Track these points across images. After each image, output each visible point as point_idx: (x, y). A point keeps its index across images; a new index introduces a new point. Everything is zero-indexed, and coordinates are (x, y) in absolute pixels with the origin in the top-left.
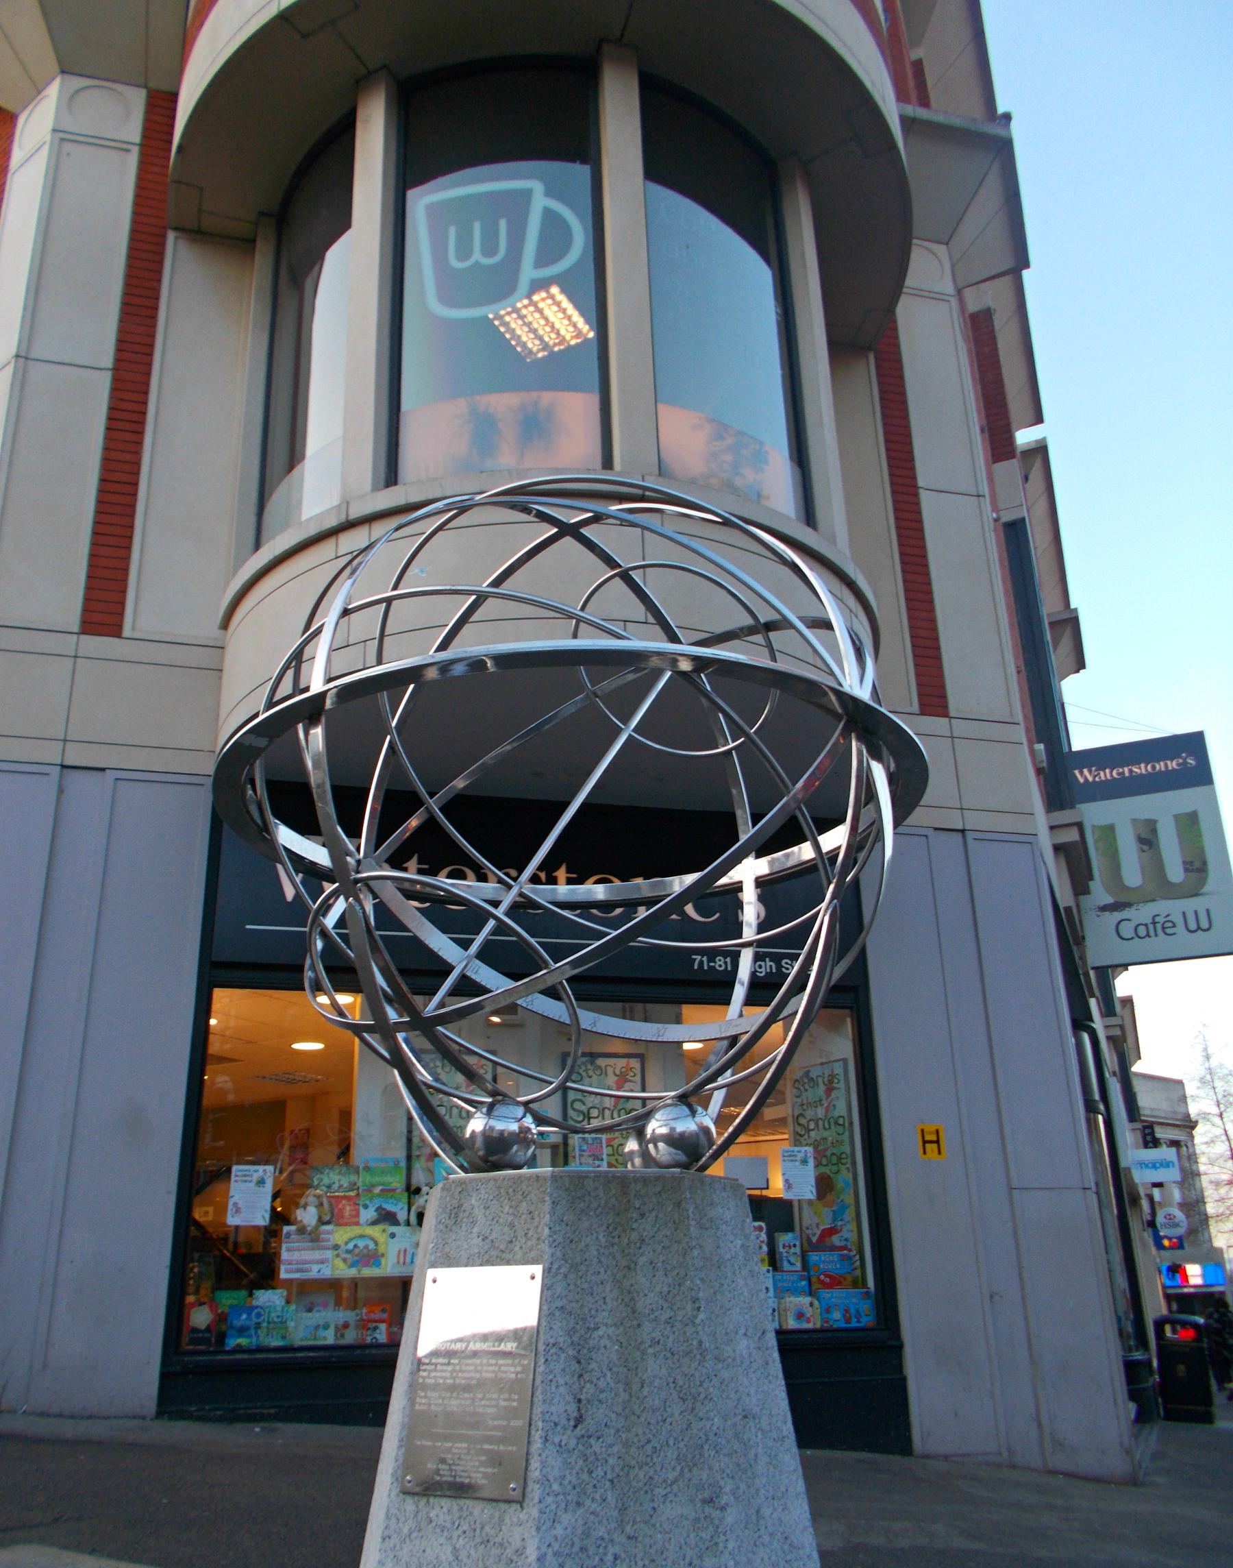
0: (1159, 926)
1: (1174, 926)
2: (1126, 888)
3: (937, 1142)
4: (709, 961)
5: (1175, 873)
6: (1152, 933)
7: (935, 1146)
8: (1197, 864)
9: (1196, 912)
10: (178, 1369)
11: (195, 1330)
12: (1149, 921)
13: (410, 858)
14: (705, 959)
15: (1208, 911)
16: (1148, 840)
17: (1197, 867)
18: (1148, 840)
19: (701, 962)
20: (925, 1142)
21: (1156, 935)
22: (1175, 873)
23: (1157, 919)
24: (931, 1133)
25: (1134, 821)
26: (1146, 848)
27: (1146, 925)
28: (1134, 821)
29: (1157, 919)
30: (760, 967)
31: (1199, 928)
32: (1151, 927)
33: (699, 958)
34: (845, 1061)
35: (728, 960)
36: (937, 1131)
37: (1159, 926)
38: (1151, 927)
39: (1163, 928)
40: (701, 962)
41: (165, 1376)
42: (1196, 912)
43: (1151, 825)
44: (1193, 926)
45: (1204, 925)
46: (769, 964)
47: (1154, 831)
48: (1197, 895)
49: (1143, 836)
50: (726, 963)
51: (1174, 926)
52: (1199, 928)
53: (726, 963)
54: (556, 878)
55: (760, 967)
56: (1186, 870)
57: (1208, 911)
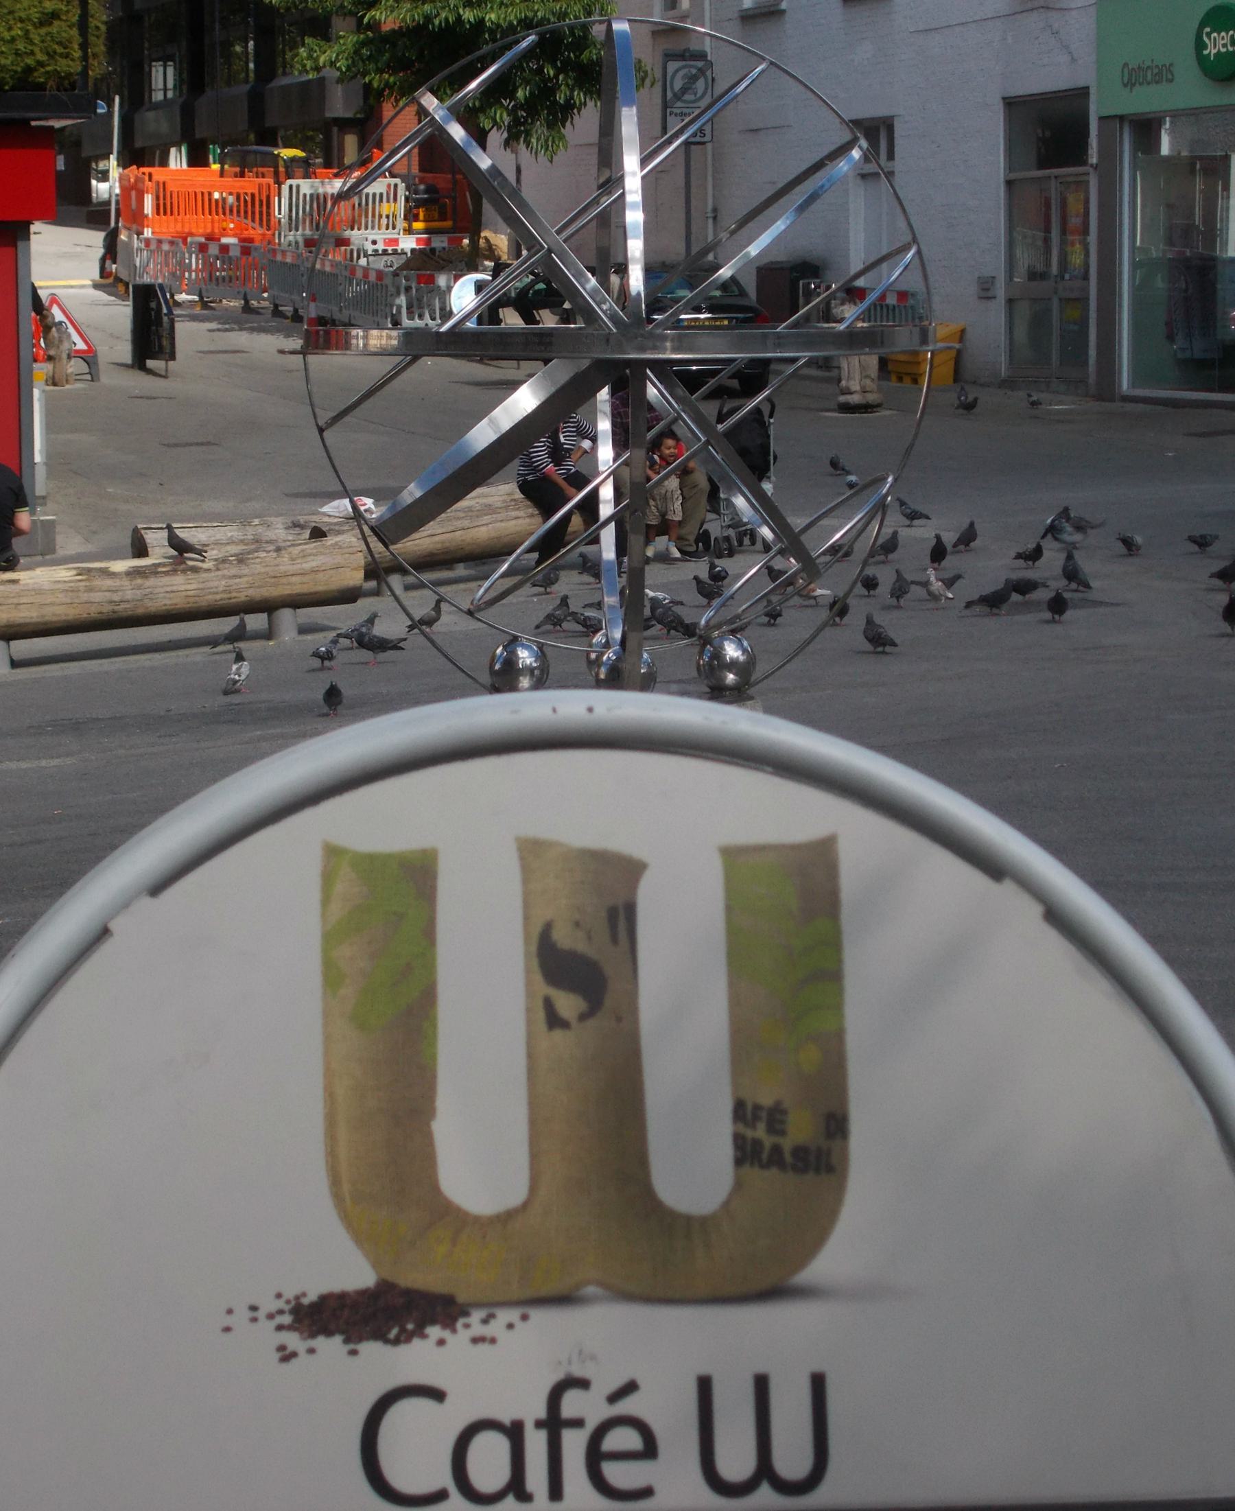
0: (574, 1444)
1: (650, 1450)
2: (445, 1213)
5: (693, 1165)
6: (537, 1478)
8: (801, 1129)
9: (761, 1385)
12: (533, 1408)
15: (818, 1383)
16: (584, 966)
17: (796, 1144)
18: (584, 966)
21: (556, 1492)
22: (693, 1165)
23: (572, 1404)
25: (532, 852)
26: (568, 1004)
27: (515, 1432)
28: (532, 852)
29: (572, 1404)
31: (765, 1471)
32: (536, 1443)
37: (574, 1444)
38: (536, 1443)
39: (595, 1457)
42: (761, 1385)
43: (612, 892)
44: (736, 1460)
45: (792, 1459)
47: (621, 919)
48: (776, 1292)
49: (564, 938)
51: (650, 1450)
52: (765, 1471)
56: (747, 1153)
57: (818, 1383)
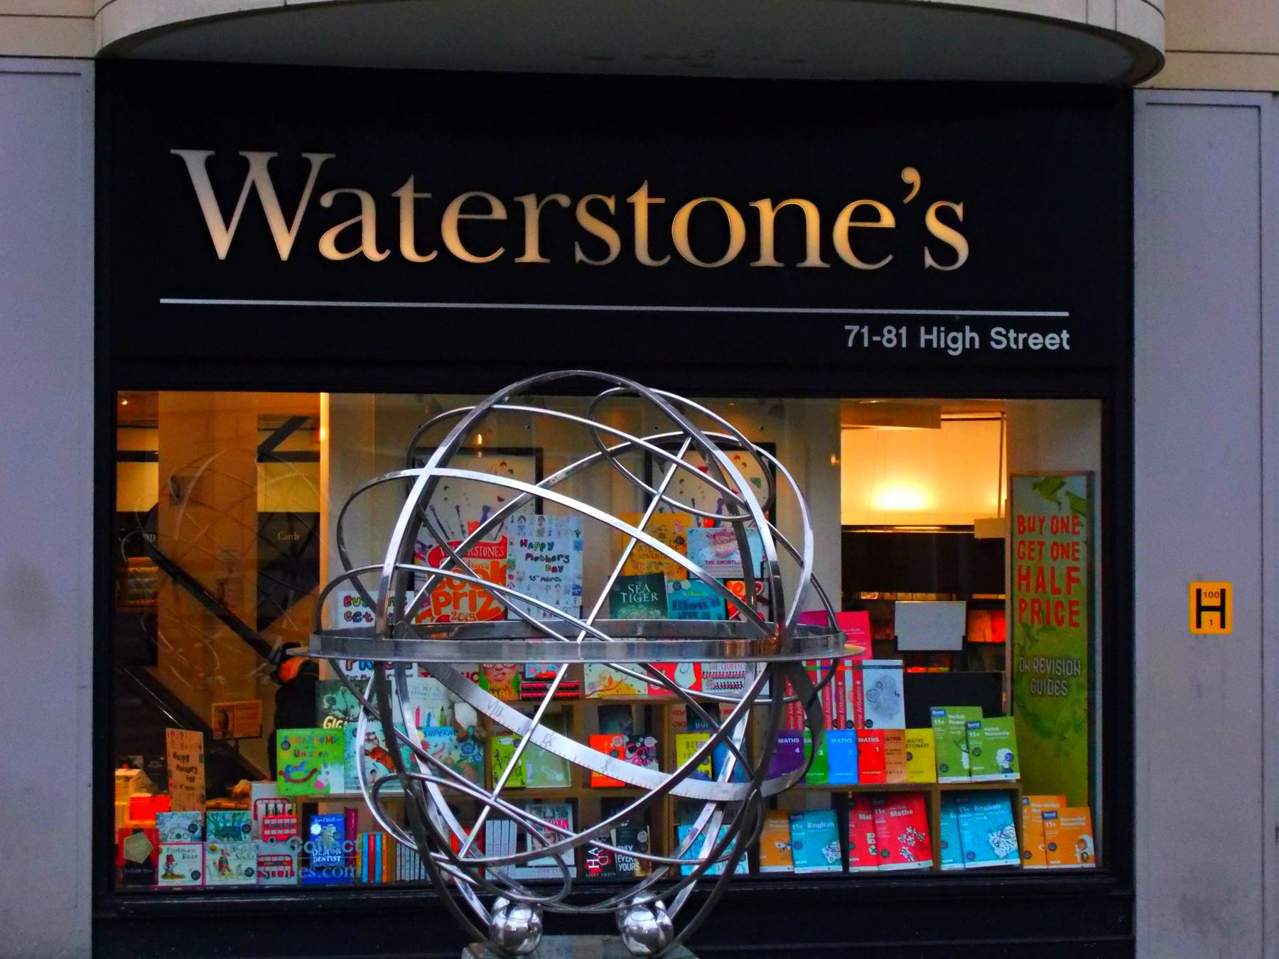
3: (1221, 609)
4: (871, 335)
7: (1217, 614)
10: (113, 915)
11: (131, 864)
13: (400, 184)
14: (865, 330)
19: (859, 336)
20: (1200, 609)
24: (1211, 595)
30: (955, 340)
33: (856, 328)
34: (1090, 475)
35: (903, 331)
36: (1223, 592)
40: (859, 336)
41: (96, 923)
46: (969, 335)
50: (898, 336)
53: (898, 336)
54: (632, 207)
55: (955, 340)
